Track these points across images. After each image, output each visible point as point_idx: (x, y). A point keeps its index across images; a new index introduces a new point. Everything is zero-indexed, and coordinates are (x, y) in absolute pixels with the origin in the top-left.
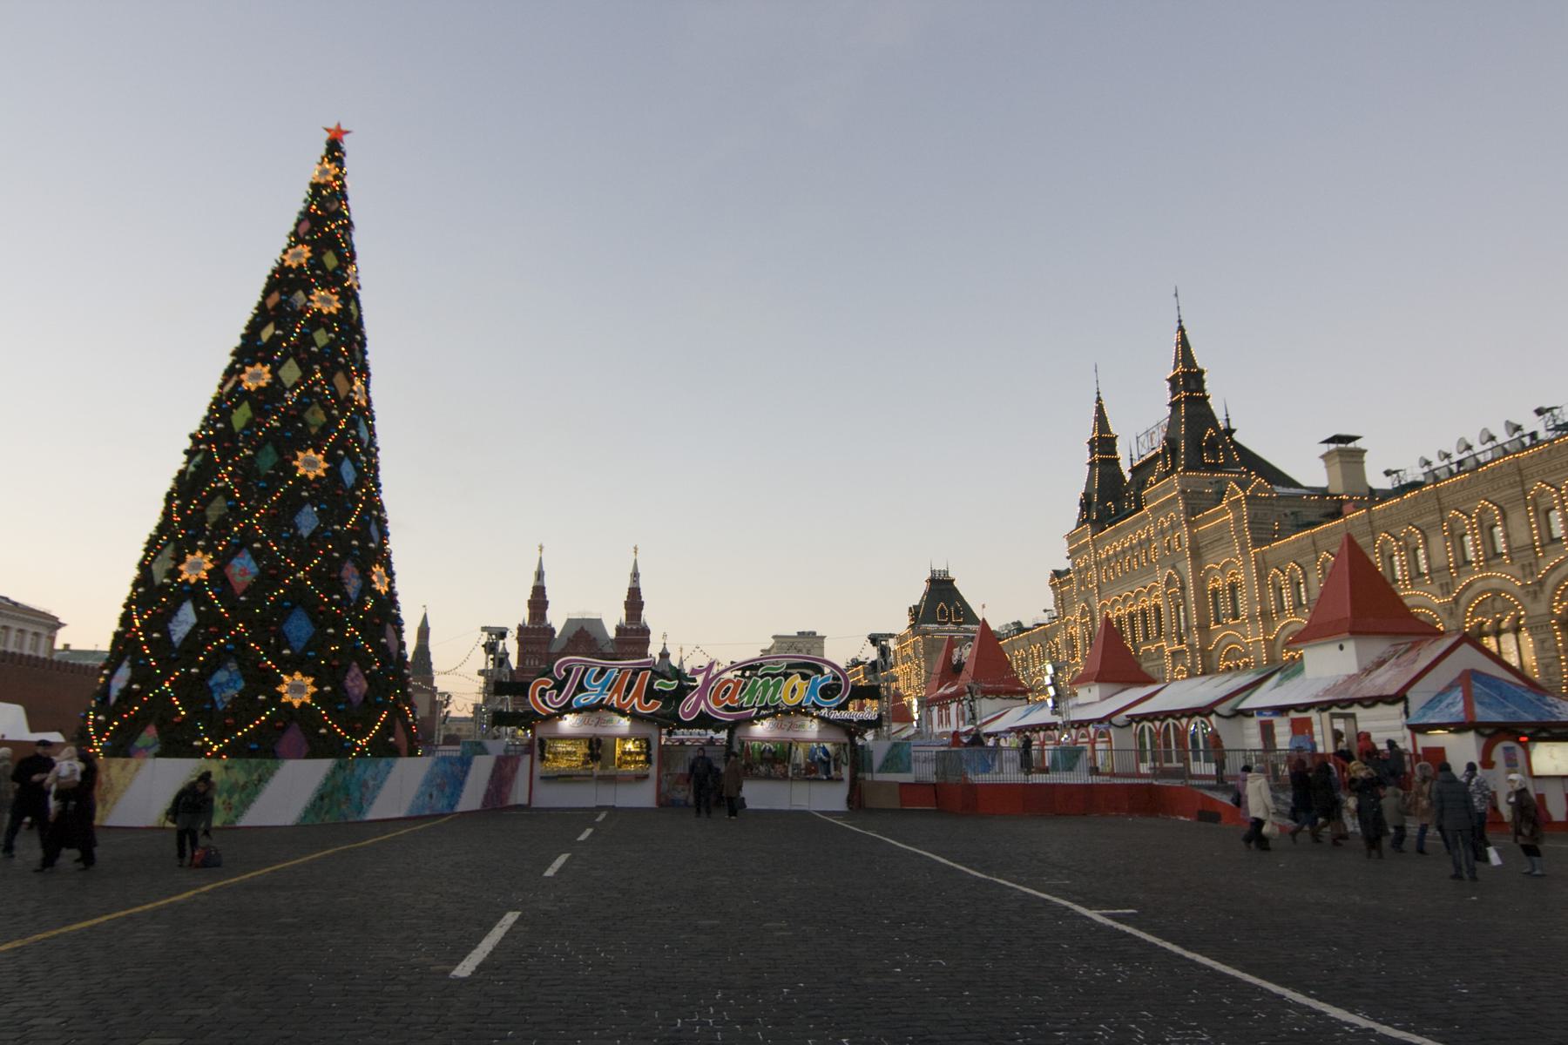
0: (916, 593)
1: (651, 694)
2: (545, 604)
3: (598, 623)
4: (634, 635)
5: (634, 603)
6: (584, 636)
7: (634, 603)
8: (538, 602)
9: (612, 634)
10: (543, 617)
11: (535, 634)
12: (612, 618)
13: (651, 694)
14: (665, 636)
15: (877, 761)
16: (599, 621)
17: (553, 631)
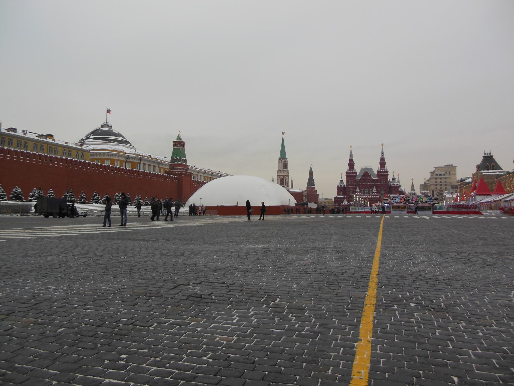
0: (479, 161)
1: (405, 200)
2: (353, 165)
3: (371, 169)
4: (383, 174)
5: (383, 163)
6: (366, 174)
7: (383, 163)
8: (351, 164)
9: (376, 173)
10: (353, 168)
11: (351, 175)
12: (376, 168)
13: (405, 200)
14: (394, 173)
15: (438, 208)
16: (371, 169)
17: (357, 173)
